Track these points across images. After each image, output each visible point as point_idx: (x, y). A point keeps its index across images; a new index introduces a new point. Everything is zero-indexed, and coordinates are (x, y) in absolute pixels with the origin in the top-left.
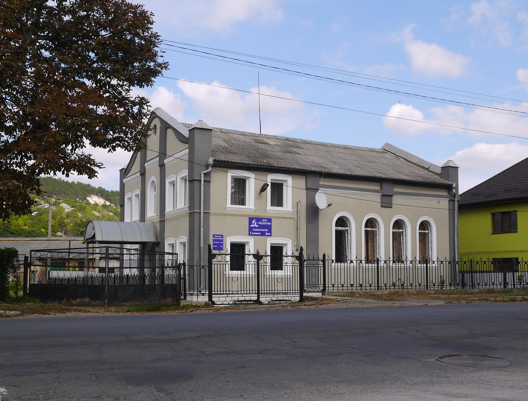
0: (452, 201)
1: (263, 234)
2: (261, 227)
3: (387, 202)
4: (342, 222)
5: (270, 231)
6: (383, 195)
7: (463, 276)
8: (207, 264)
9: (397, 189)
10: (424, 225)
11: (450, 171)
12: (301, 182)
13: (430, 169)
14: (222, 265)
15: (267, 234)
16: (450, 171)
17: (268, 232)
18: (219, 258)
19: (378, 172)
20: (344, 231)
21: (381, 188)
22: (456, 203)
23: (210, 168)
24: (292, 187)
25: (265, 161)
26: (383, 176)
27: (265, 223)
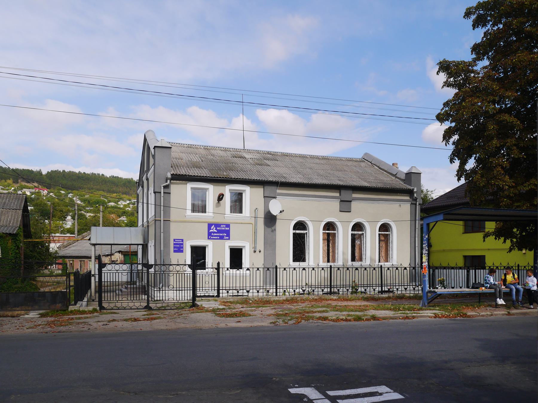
0: (413, 204)
1: (222, 238)
2: (219, 232)
3: (345, 206)
4: (300, 225)
5: (228, 235)
6: (341, 201)
7: (434, 271)
8: (97, 272)
9: (355, 195)
10: (385, 227)
11: (412, 177)
12: (259, 191)
13: (397, 176)
14: (111, 274)
15: (225, 238)
16: (412, 177)
17: (226, 236)
18: (109, 267)
19: (339, 180)
20: (304, 234)
21: (340, 195)
22: (418, 207)
23: (169, 181)
24: (251, 196)
25: (224, 174)
26: (341, 183)
27: (223, 229)
